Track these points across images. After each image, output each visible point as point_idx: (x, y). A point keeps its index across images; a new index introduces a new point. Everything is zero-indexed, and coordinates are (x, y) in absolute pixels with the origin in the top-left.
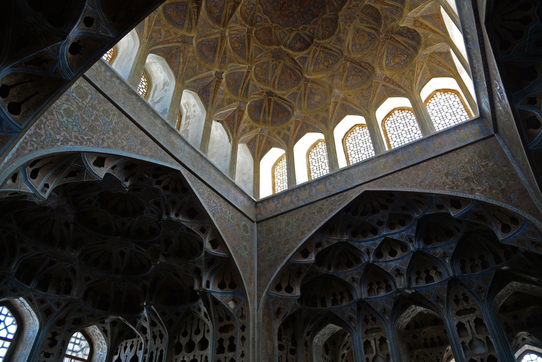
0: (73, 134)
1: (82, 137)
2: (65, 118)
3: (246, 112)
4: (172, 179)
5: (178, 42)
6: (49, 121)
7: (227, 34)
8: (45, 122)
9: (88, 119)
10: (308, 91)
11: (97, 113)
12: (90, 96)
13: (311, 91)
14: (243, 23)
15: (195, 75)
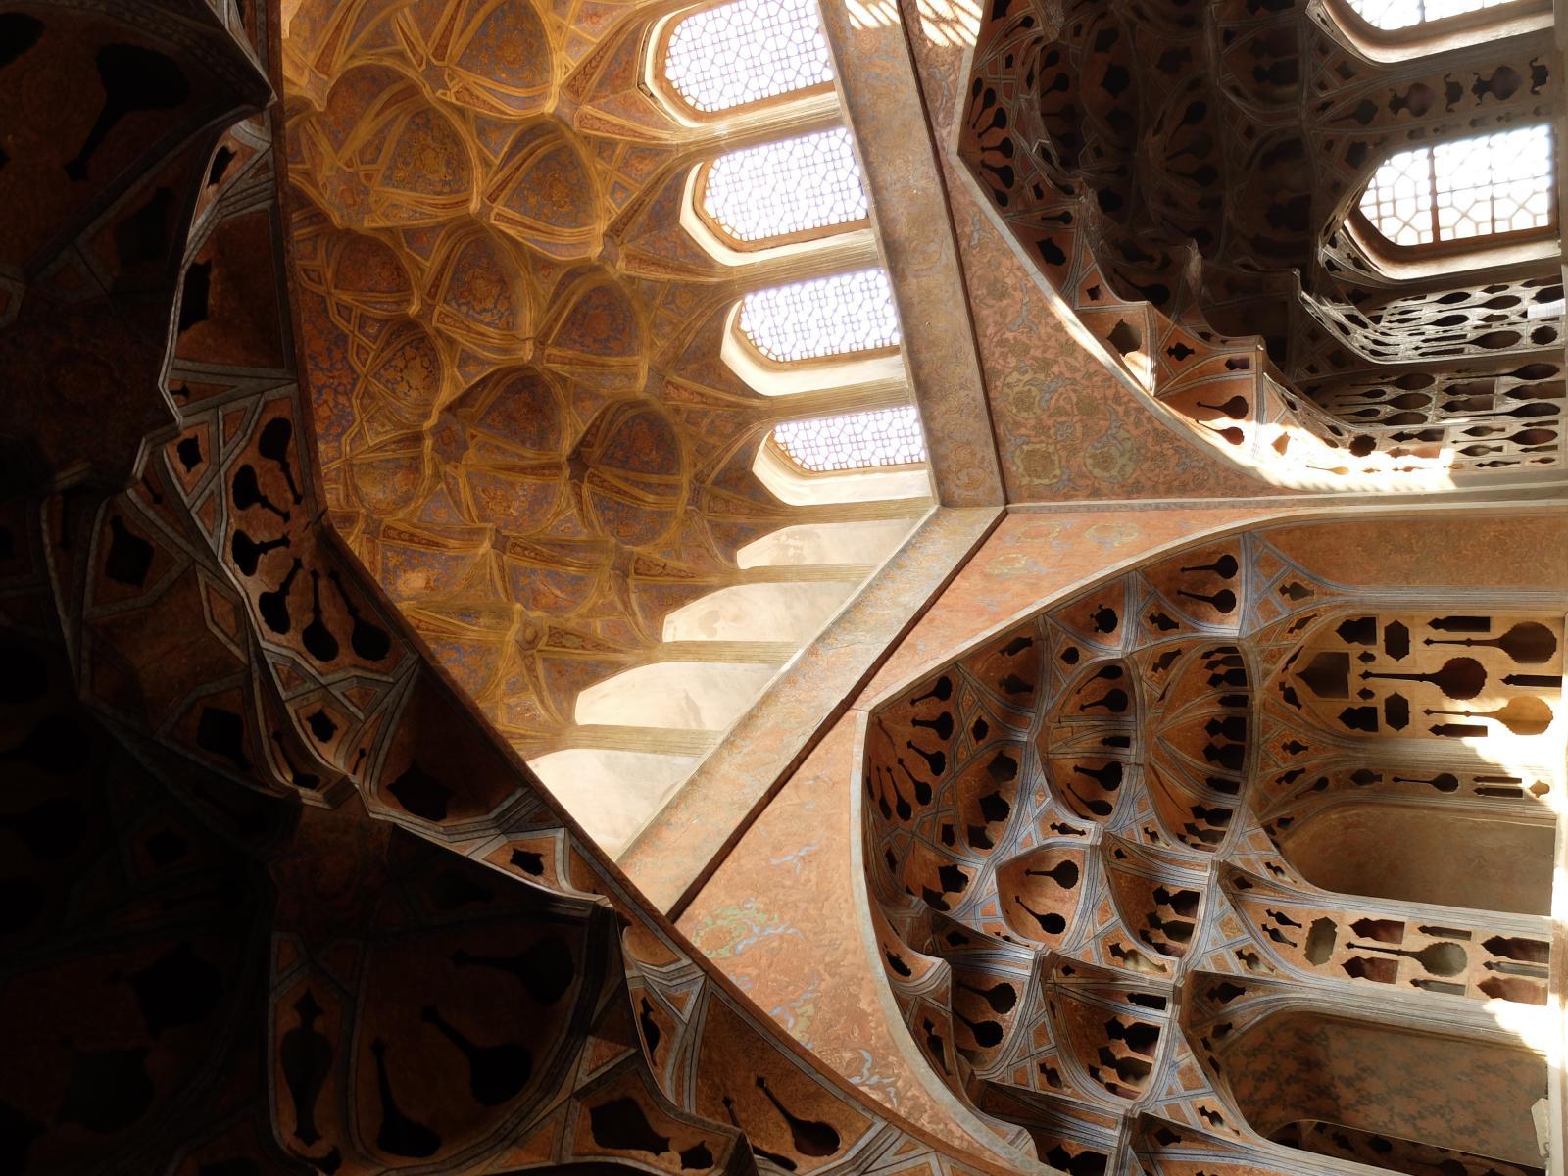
0: (1135, 433)
1: (1127, 413)
2: (1121, 461)
3: (558, 78)
4: (980, 136)
5: (677, 387)
6: (1156, 479)
7: (529, 345)
8: (1164, 483)
9: (1078, 426)
10: (325, 37)
11: (1044, 417)
12: (1025, 447)
13: (313, 31)
14: (440, 343)
15: (676, 285)
